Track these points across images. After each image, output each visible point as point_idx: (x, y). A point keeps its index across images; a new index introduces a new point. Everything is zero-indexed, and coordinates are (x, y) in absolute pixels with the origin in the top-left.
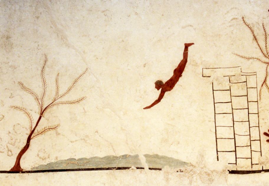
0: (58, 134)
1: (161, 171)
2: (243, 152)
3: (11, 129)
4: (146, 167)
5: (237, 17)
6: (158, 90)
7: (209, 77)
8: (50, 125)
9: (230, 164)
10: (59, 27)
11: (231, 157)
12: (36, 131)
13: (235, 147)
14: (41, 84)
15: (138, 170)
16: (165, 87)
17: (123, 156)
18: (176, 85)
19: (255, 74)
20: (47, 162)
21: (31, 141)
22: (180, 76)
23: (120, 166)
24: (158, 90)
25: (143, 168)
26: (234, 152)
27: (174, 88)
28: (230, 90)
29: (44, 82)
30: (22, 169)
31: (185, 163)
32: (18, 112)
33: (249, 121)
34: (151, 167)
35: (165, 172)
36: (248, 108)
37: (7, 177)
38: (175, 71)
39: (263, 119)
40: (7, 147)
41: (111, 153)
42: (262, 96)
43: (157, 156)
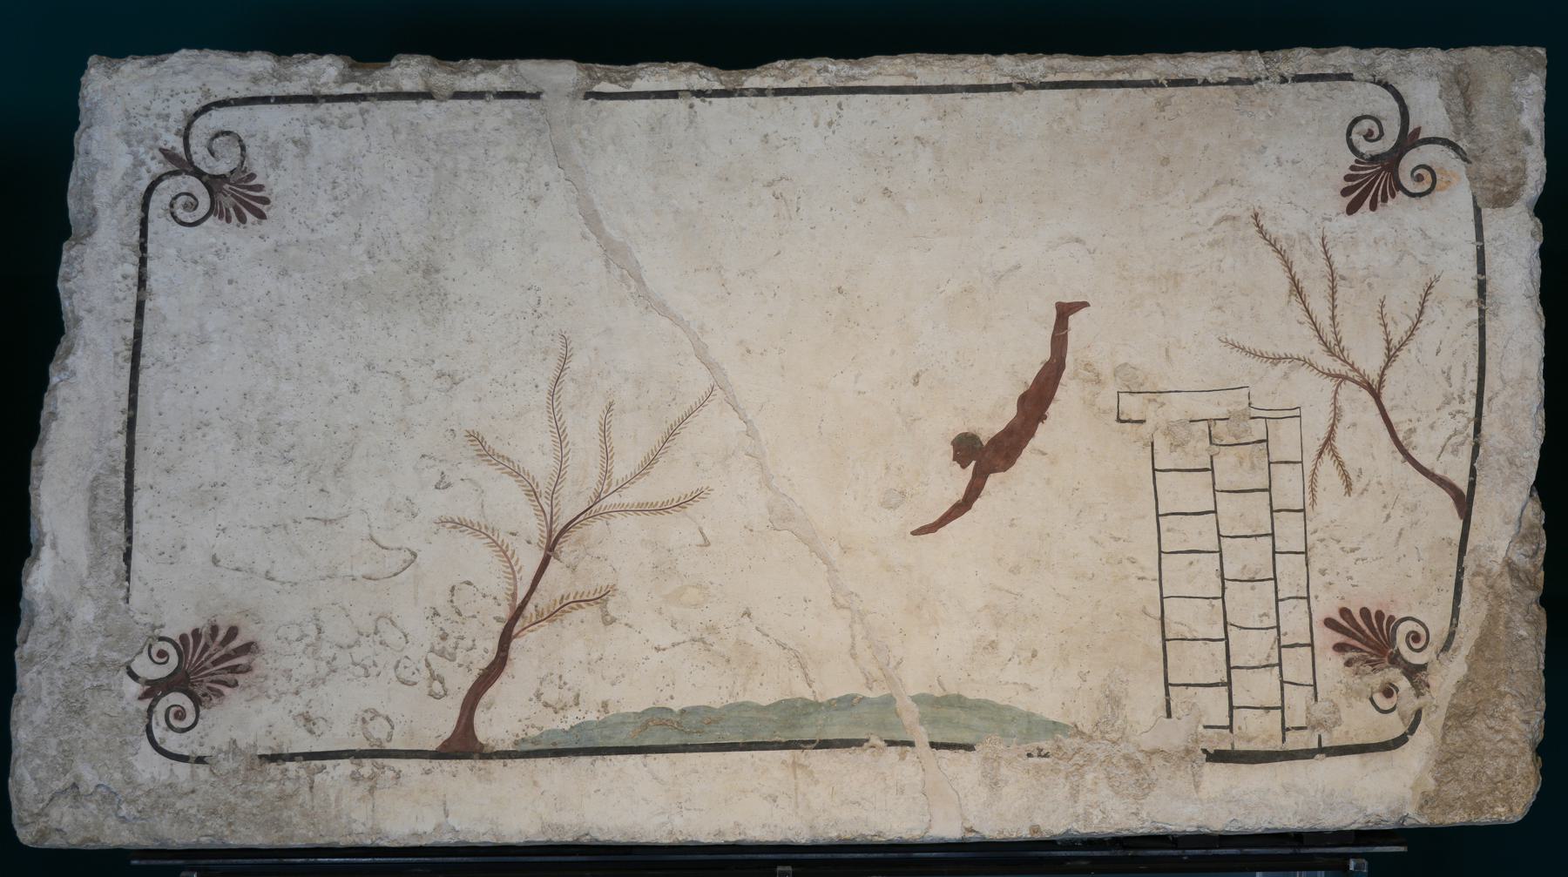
0: (608, 621)
1: (970, 754)
2: (1257, 687)
3: (441, 602)
4: (922, 736)
5: (1235, 212)
6: (964, 467)
7: (1142, 422)
8: (580, 587)
9: (1210, 731)
10: (614, 234)
11: (1213, 706)
12: (530, 607)
13: (1229, 668)
14: (548, 441)
15: (893, 749)
16: (988, 456)
17: (839, 700)
18: (1026, 452)
19: (1296, 412)
20: (572, 718)
21: (515, 644)
22: (1042, 417)
23: (833, 733)
24: (964, 467)
25: (911, 744)
26: (1224, 689)
27: (1019, 460)
28: (1212, 470)
29: (561, 437)
30: (482, 746)
31: (1054, 727)
32: (466, 539)
33: (1275, 579)
34: (938, 739)
35: (986, 759)
36: (1273, 534)
37: (428, 772)
38: (1023, 399)
39: (1323, 572)
40: (428, 665)
41: (802, 691)
42: (1319, 489)
43: (957, 702)
